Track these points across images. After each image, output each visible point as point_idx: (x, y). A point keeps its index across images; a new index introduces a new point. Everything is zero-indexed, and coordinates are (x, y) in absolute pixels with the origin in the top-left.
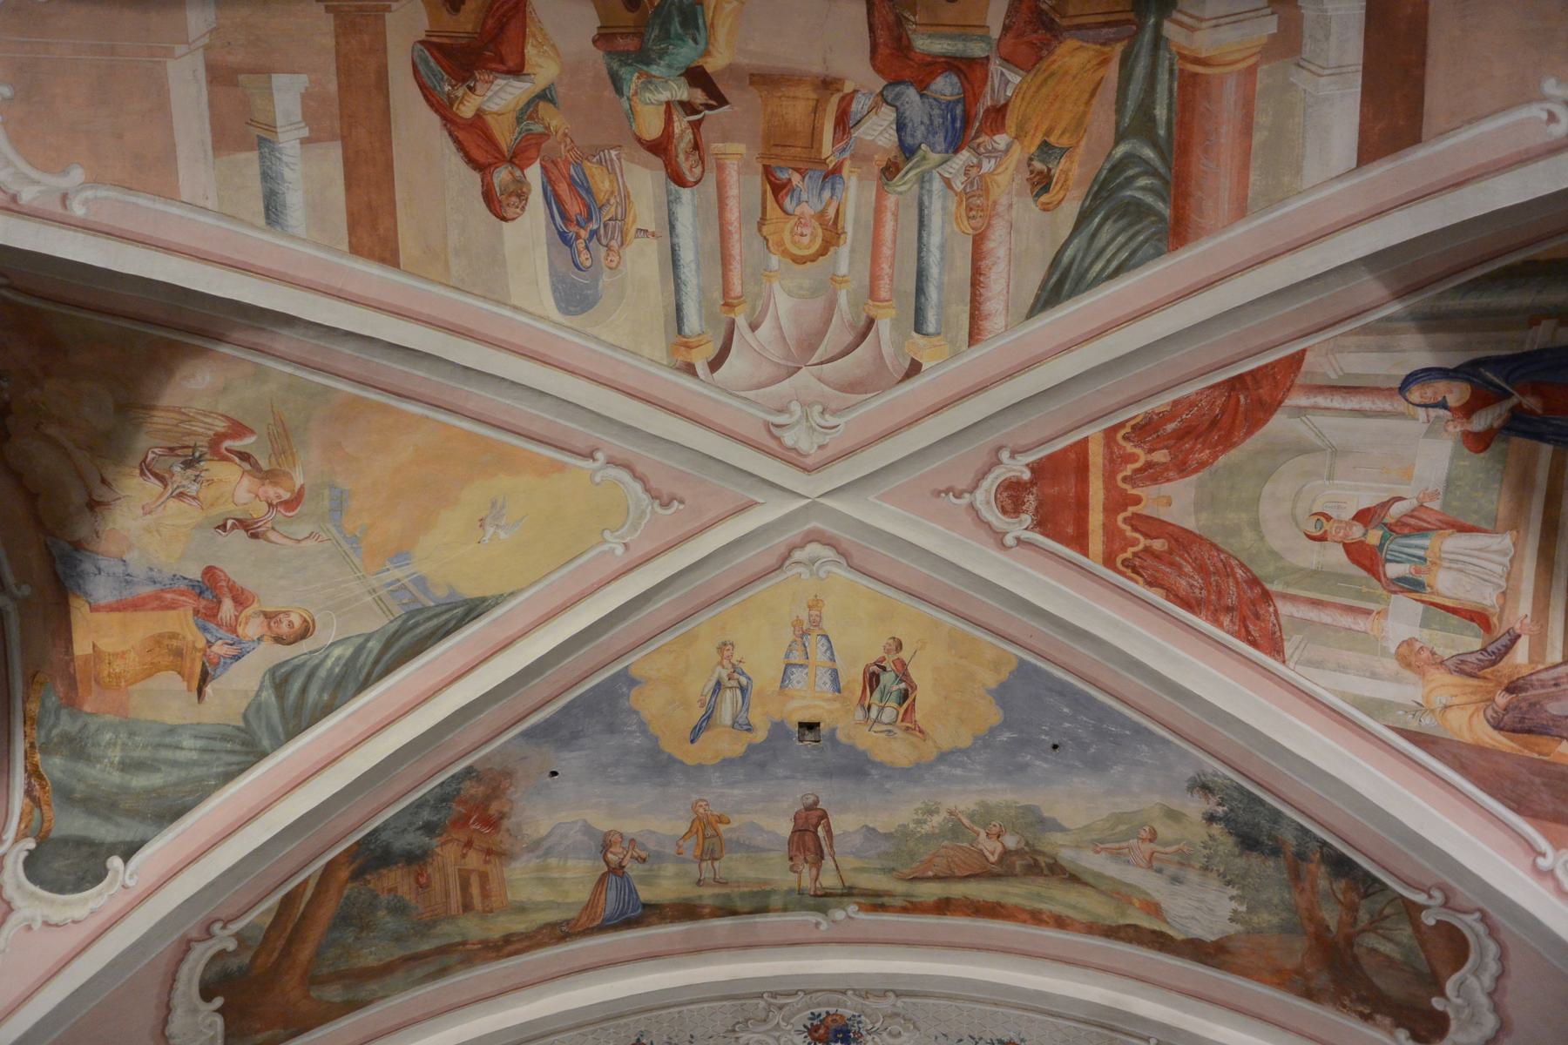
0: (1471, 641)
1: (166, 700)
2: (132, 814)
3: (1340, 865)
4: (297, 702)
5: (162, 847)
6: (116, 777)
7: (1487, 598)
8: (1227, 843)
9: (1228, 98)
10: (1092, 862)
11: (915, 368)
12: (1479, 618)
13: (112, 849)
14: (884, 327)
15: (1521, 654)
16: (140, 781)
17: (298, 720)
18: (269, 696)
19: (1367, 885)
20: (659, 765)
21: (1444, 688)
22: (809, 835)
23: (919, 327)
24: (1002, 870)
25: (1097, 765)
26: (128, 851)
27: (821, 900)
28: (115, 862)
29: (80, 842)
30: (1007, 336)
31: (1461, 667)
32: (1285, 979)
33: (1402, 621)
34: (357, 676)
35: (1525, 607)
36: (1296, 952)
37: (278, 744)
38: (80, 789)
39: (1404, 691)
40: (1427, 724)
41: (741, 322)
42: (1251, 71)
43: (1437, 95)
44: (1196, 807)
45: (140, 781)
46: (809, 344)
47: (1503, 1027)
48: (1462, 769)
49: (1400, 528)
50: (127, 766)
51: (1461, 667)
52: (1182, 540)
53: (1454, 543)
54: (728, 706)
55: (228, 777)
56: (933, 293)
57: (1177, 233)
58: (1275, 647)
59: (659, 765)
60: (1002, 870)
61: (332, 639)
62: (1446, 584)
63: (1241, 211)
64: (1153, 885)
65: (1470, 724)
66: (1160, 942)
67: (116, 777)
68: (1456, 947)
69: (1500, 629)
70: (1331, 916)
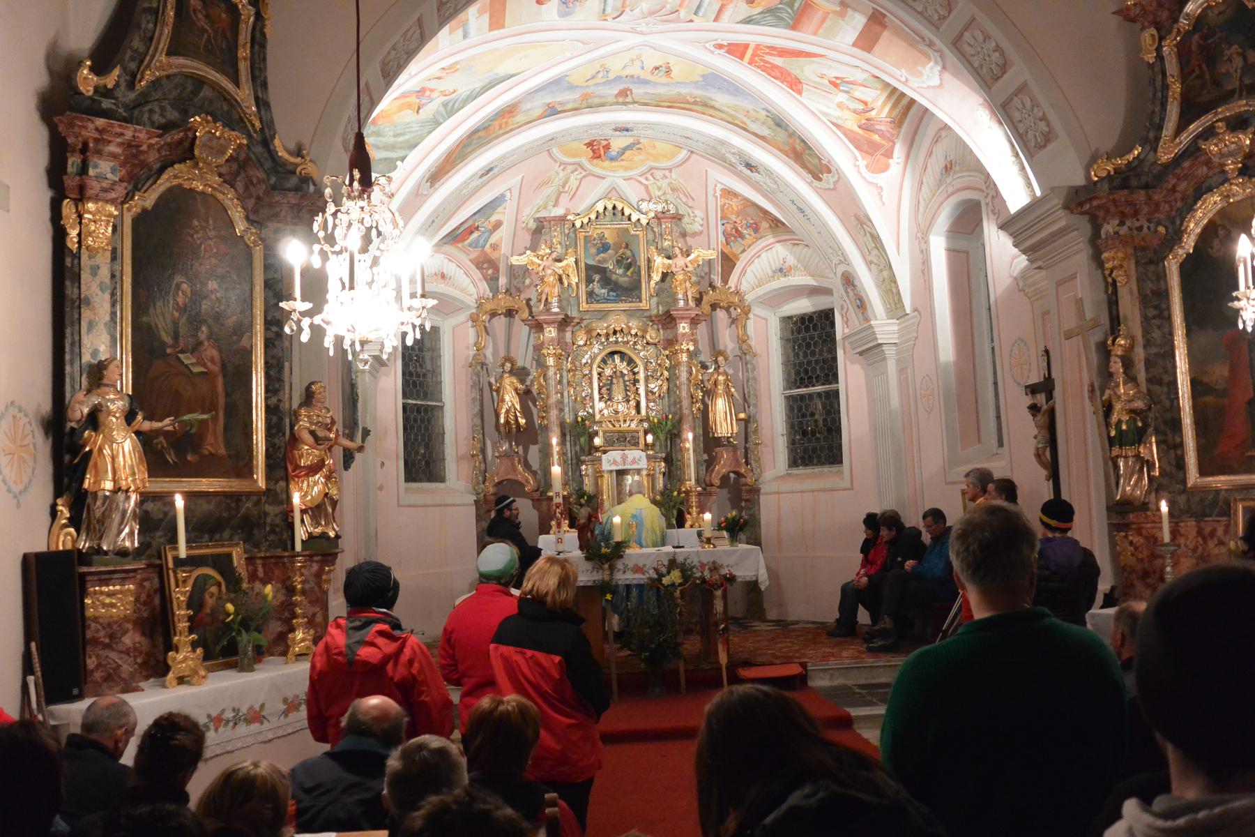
0: (861, 106)
1: (409, 116)
2: (401, 148)
3: (803, 141)
4: (450, 109)
5: (413, 156)
6: (393, 139)
7: (869, 100)
8: (770, 122)
9: (819, 15)
10: (725, 109)
11: (691, 21)
12: (865, 103)
13: (397, 159)
14: (682, 13)
15: (873, 114)
16: (400, 139)
17: (451, 113)
18: (442, 109)
19: (810, 148)
20: (572, 87)
21: (848, 115)
22: (624, 93)
23: (696, 13)
24: (695, 103)
25: (734, 95)
26: (403, 159)
27: (625, 104)
28: (399, 163)
29: (385, 159)
30: (725, 22)
31: (855, 112)
32: (780, 150)
33: (842, 97)
34: (472, 97)
35: (879, 103)
36: (787, 148)
37: (445, 120)
38: (381, 145)
39: (836, 113)
40: (839, 122)
41: (627, 10)
42: (828, 13)
43: (877, 48)
44: (764, 113)
45: (400, 139)
46: (652, 13)
47: (835, 189)
48: (845, 135)
49: (848, 83)
50: (394, 136)
51: (855, 112)
52: (774, 66)
53: (862, 88)
54: (601, 75)
55: (430, 132)
56: (703, 10)
57: (794, 27)
58: (800, 93)
59: (572, 87)
60: (695, 103)
61: (463, 91)
62: (857, 94)
63: (815, 34)
64: (746, 120)
65: (852, 123)
66: (745, 129)
67: (393, 139)
68: (829, 171)
69: (870, 106)
70: (798, 148)
